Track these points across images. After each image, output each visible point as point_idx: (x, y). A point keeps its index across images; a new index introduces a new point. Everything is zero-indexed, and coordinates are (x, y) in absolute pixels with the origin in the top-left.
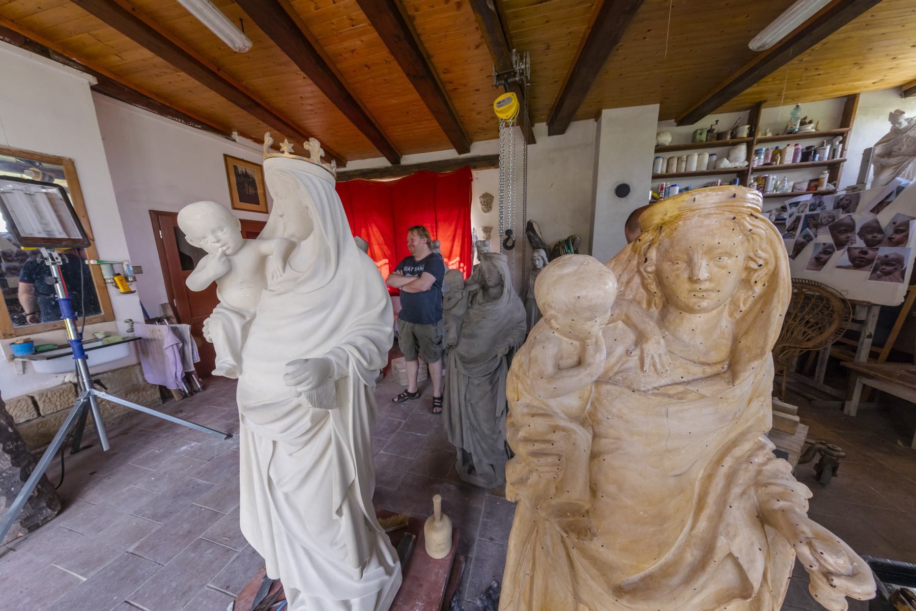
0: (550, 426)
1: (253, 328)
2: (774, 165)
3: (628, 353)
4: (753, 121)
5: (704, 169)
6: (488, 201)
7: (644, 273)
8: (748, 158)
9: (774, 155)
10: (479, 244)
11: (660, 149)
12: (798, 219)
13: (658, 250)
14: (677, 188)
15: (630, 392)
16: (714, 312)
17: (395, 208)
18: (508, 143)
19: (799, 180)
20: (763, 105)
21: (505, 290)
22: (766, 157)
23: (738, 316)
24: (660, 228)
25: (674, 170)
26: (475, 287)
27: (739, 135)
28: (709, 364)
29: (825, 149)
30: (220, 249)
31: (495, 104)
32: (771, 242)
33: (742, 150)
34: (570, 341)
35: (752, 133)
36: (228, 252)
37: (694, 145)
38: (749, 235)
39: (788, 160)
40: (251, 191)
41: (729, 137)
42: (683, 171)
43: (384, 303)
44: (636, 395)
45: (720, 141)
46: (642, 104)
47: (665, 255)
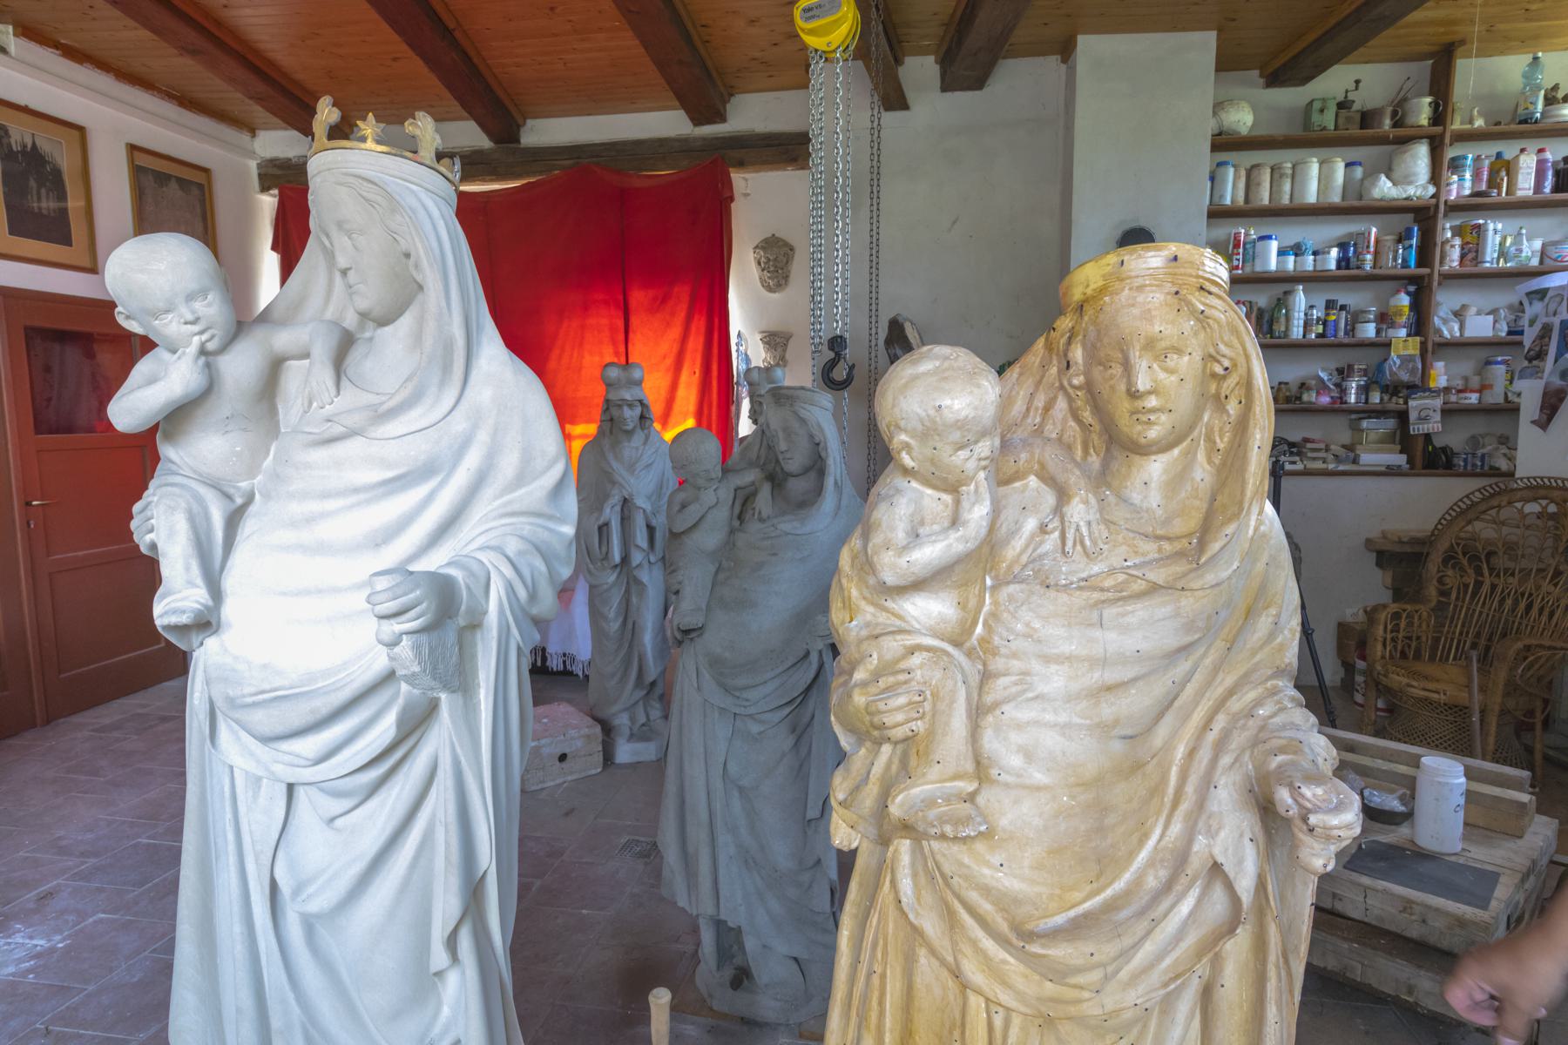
0: (905, 647)
1: (248, 526)
3: (1043, 529)
4: (1440, 86)
5: (1336, 198)
6: (777, 260)
7: (1070, 390)
8: (1435, 178)
9: (1494, 173)
10: (755, 376)
11: (1225, 143)
12: (1546, 330)
13: (1084, 348)
14: (1274, 246)
15: (1043, 590)
16: (1176, 451)
17: (587, 258)
18: (833, 107)
19: (1556, 238)
20: (1460, 51)
21: (829, 482)
22: (1476, 176)
23: (1217, 460)
24: (1081, 308)
25: (1264, 197)
26: (750, 476)
27: (1410, 120)
28: (1168, 539)
30: (196, 339)
31: (797, 13)
32: (1235, 331)
33: (1419, 159)
34: (936, 494)
35: (1439, 118)
36: (211, 346)
37: (1307, 138)
38: (1202, 317)
39: (1525, 185)
40: (48, 204)
41: (1387, 122)
42: (1286, 200)
43: (559, 468)
44: (1052, 593)
45: (1369, 131)
46: (1174, 28)
47: (1092, 356)
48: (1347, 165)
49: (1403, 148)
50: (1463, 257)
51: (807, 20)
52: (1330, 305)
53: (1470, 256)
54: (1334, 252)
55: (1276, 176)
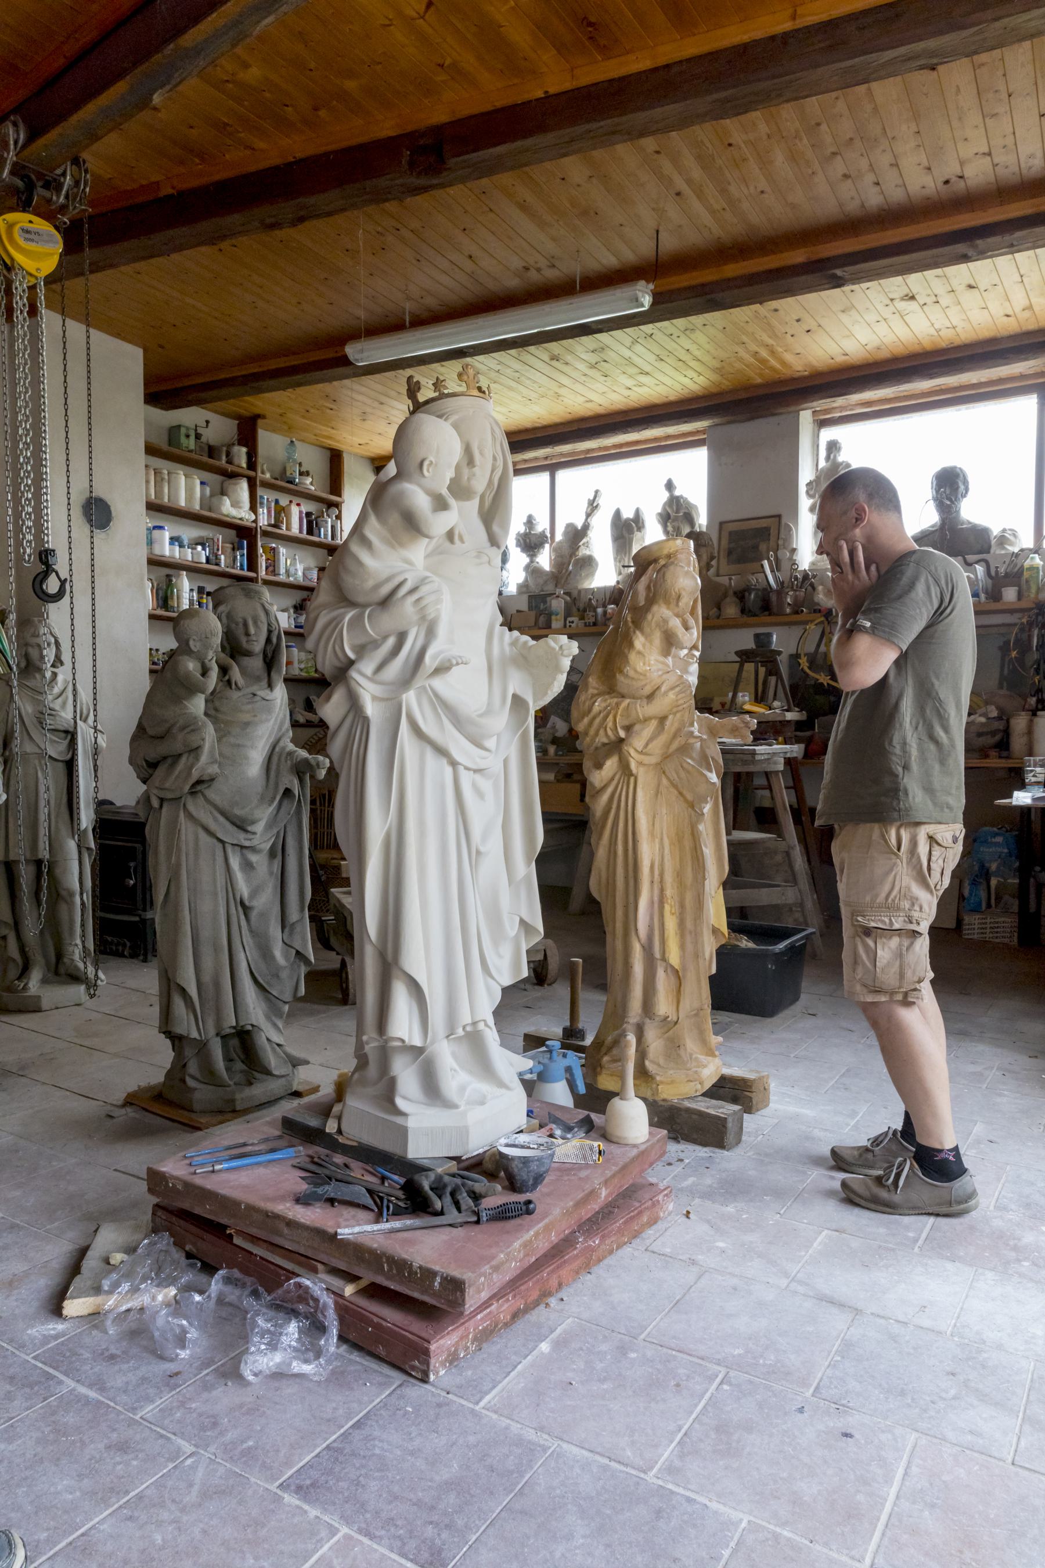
2: (283, 531)
5: (196, 507)
8: (253, 508)
20: (260, 422)
22: (269, 512)
27: (236, 461)
29: (327, 522)
35: (252, 465)
41: (224, 458)
48: (202, 483)
49: (233, 481)
50: (267, 568)
51: (26, 239)
52: (201, 590)
53: (271, 569)
54: (199, 548)
55: (158, 479)
